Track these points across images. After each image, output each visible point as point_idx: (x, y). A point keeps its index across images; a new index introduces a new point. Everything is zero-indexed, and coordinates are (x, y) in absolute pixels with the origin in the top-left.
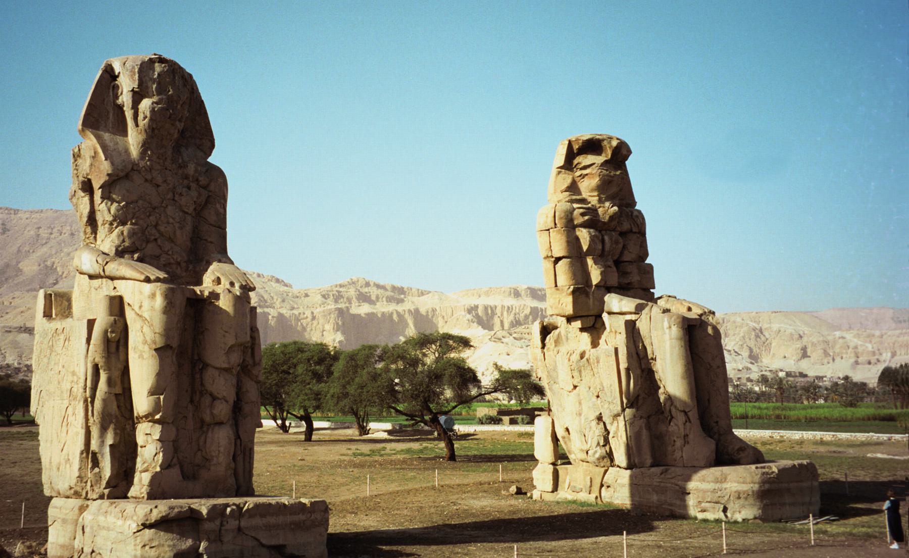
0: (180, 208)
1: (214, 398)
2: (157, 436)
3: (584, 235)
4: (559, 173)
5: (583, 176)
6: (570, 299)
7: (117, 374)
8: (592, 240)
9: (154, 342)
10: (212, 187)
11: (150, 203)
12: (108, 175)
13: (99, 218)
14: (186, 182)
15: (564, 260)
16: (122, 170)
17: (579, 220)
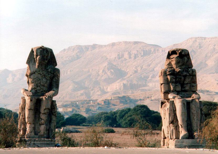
0: (46, 79)
1: (42, 119)
2: (29, 126)
3: (169, 77)
4: (167, 60)
5: (172, 61)
6: (163, 95)
7: (23, 114)
8: (171, 79)
9: (28, 108)
10: (55, 74)
11: (39, 79)
12: (30, 73)
13: (30, 82)
14: (48, 73)
15: (163, 85)
16: (33, 72)
17: (168, 73)
